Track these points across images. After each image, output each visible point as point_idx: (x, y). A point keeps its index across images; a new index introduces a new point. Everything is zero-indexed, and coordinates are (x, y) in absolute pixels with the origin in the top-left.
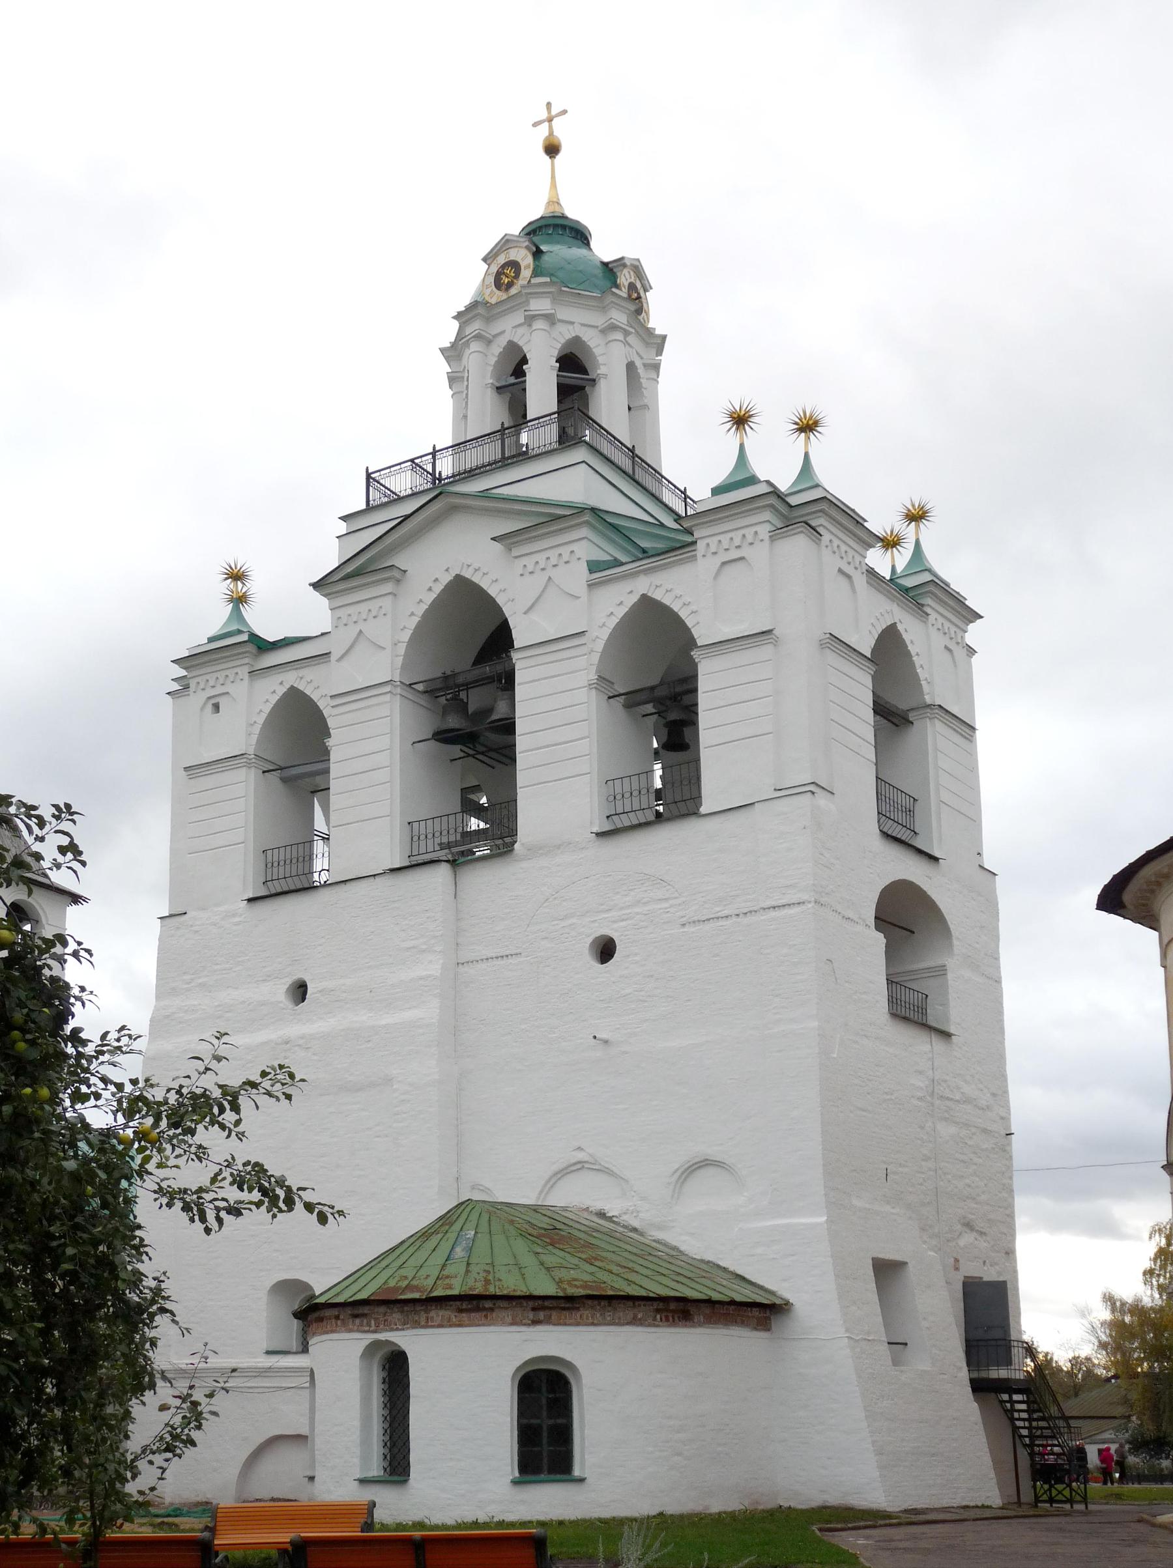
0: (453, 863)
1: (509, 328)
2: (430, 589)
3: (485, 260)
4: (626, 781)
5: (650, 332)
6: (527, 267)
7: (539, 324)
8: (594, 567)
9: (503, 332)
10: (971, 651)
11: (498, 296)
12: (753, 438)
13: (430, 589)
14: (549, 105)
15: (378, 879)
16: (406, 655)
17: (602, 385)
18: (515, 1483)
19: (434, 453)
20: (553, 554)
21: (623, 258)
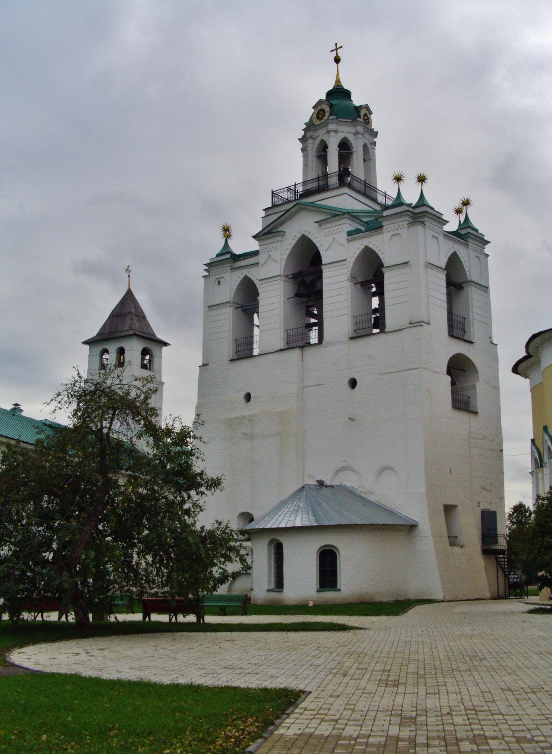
1: (321, 134)
2: (293, 239)
3: (313, 108)
4: (361, 317)
5: (372, 130)
6: (327, 112)
7: (332, 134)
8: (350, 234)
9: (319, 136)
10: (487, 256)
11: (317, 122)
13: (293, 239)
14: (336, 44)
15: (275, 353)
16: (285, 265)
17: (355, 155)
18: (318, 591)
19: (295, 185)
20: (335, 228)
21: (361, 105)
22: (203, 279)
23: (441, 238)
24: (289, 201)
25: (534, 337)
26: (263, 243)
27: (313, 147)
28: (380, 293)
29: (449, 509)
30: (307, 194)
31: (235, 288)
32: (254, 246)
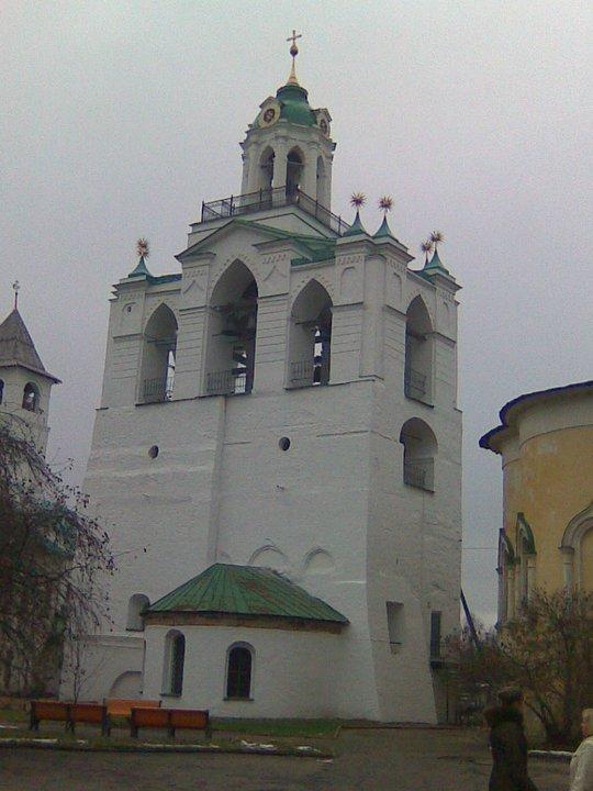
0: (226, 396)
7: (281, 140)
11: (263, 124)
12: (362, 209)
17: (306, 169)
18: (225, 700)
19: (232, 199)
23: (404, 277)
24: (222, 218)
25: (509, 405)
27: (255, 154)
28: (326, 339)
29: (393, 609)
30: (247, 210)
31: (148, 317)
32: (176, 268)
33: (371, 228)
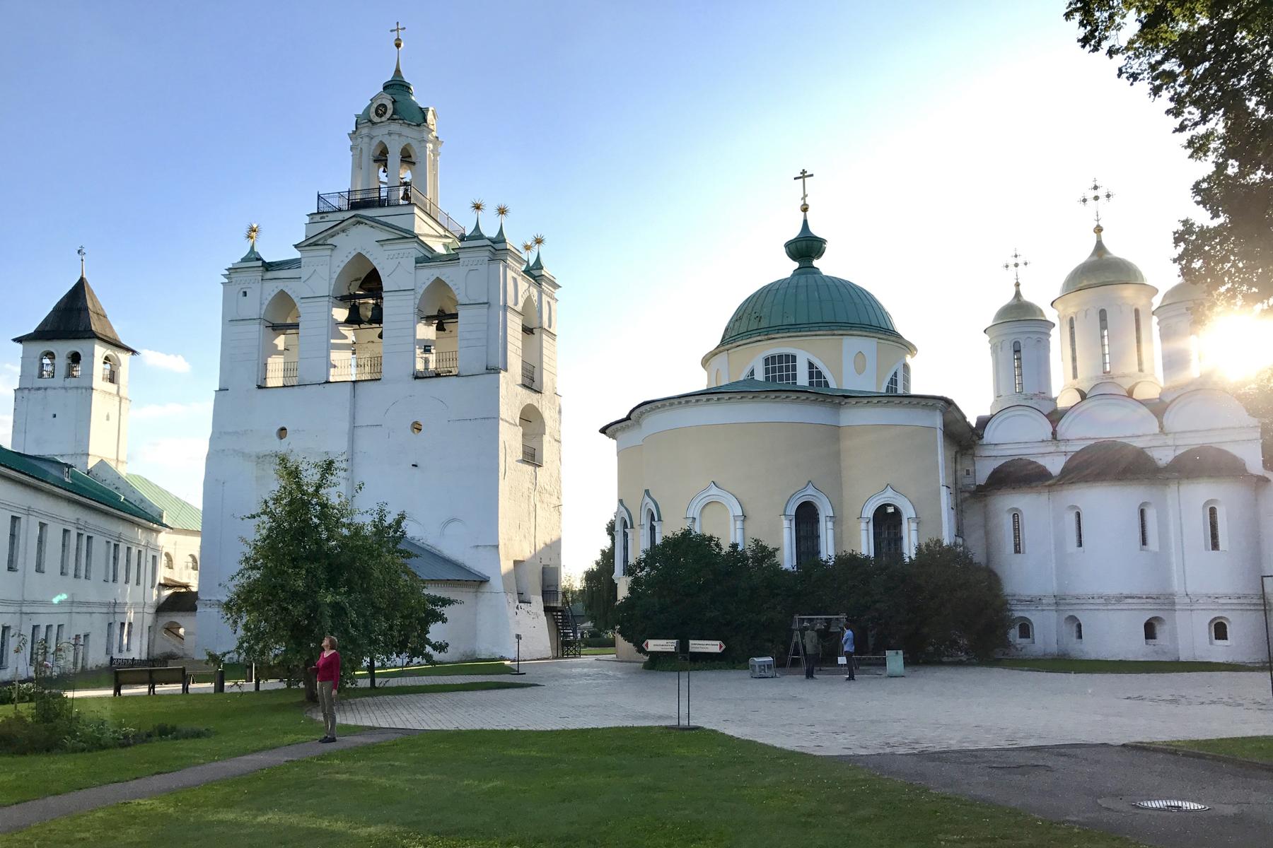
1: (381, 133)
22: (222, 286)
26: (306, 254)
27: (370, 149)
32: (296, 254)
33: (490, 231)
